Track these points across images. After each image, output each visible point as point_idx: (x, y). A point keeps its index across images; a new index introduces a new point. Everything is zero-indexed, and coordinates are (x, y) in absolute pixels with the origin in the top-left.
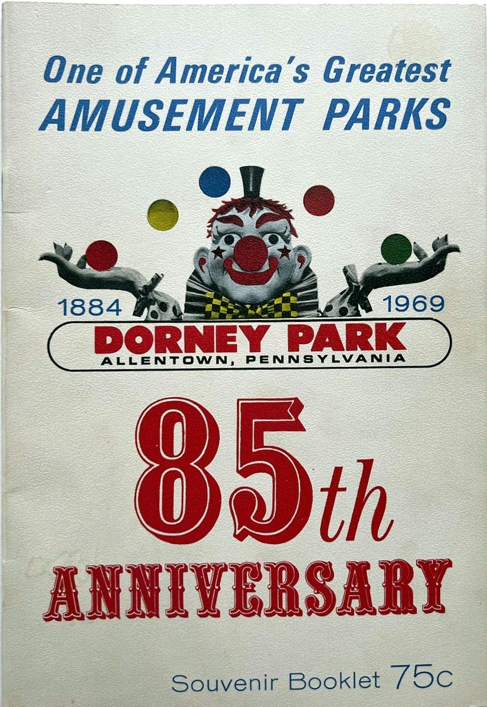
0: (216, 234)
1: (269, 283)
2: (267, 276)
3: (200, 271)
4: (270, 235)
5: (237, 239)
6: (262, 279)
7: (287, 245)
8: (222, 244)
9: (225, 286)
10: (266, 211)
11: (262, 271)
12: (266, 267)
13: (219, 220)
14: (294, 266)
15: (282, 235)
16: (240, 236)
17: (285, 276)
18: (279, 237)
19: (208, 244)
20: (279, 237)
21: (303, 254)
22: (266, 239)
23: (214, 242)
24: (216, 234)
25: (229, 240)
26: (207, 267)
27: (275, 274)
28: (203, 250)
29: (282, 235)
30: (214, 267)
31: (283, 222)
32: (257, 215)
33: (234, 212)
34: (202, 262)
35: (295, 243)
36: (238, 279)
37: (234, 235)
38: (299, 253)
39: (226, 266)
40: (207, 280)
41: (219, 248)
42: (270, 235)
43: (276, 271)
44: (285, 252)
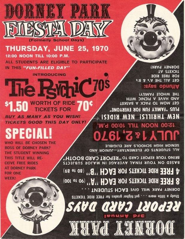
0: (137, 31)
1: (157, 50)
2: (157, 48)
3: (130, 45)
4: (158, 31)
5: (145, 32)
6: (155, 49)
7: (165, 35)
8: (139, 35)
9: (140, 52)
10: (157, 22)
11: (154, 46)
12: (157, 44)
13: (138, 25)
14: (167, 44)
15: (163, 31)
16: (146, 31)
17: (164, 48)
18: (162, 32)
19: (133, 34)
20: (162, 32)
21: (171, 39)
22: (156, 33)
23: (136, 34)
24: (137, 31)
25: (142, 33)
26: (133, 43)
27: (160, 47)
28: (131, 37)
29: (163, 31)
30: (136, 44)
31: (163, 26)
32: (153, 24)
33: (144, 22)
34: (131, 41)
35: (168, 34)
36: (146, 48)
37: (143, 31)
38: (170, 38)
39: (141, 43)
40: (133, 49)
41: (138, 36)
42: (158, 31)
43: (160, 46)
44: (164, 38)
